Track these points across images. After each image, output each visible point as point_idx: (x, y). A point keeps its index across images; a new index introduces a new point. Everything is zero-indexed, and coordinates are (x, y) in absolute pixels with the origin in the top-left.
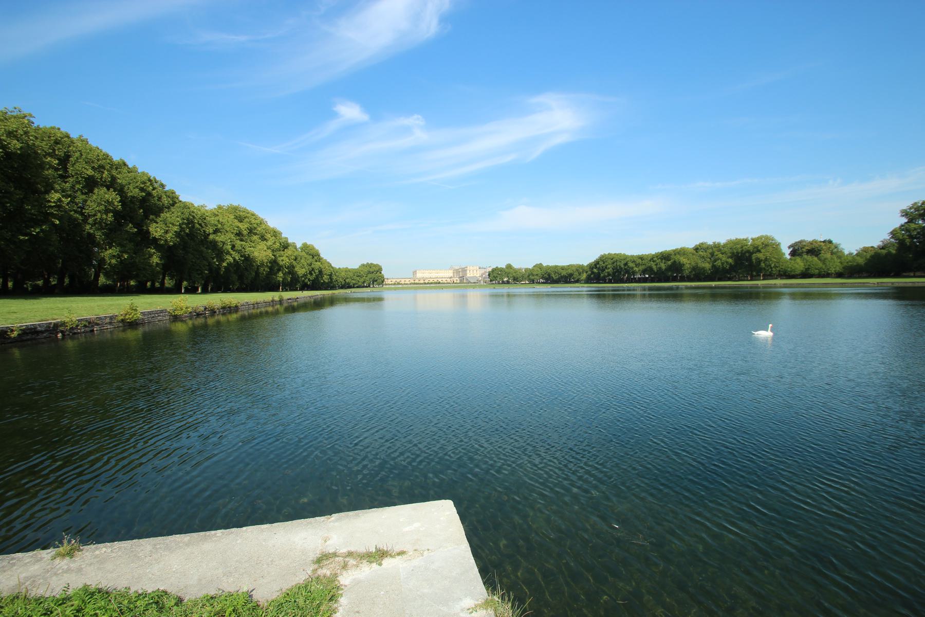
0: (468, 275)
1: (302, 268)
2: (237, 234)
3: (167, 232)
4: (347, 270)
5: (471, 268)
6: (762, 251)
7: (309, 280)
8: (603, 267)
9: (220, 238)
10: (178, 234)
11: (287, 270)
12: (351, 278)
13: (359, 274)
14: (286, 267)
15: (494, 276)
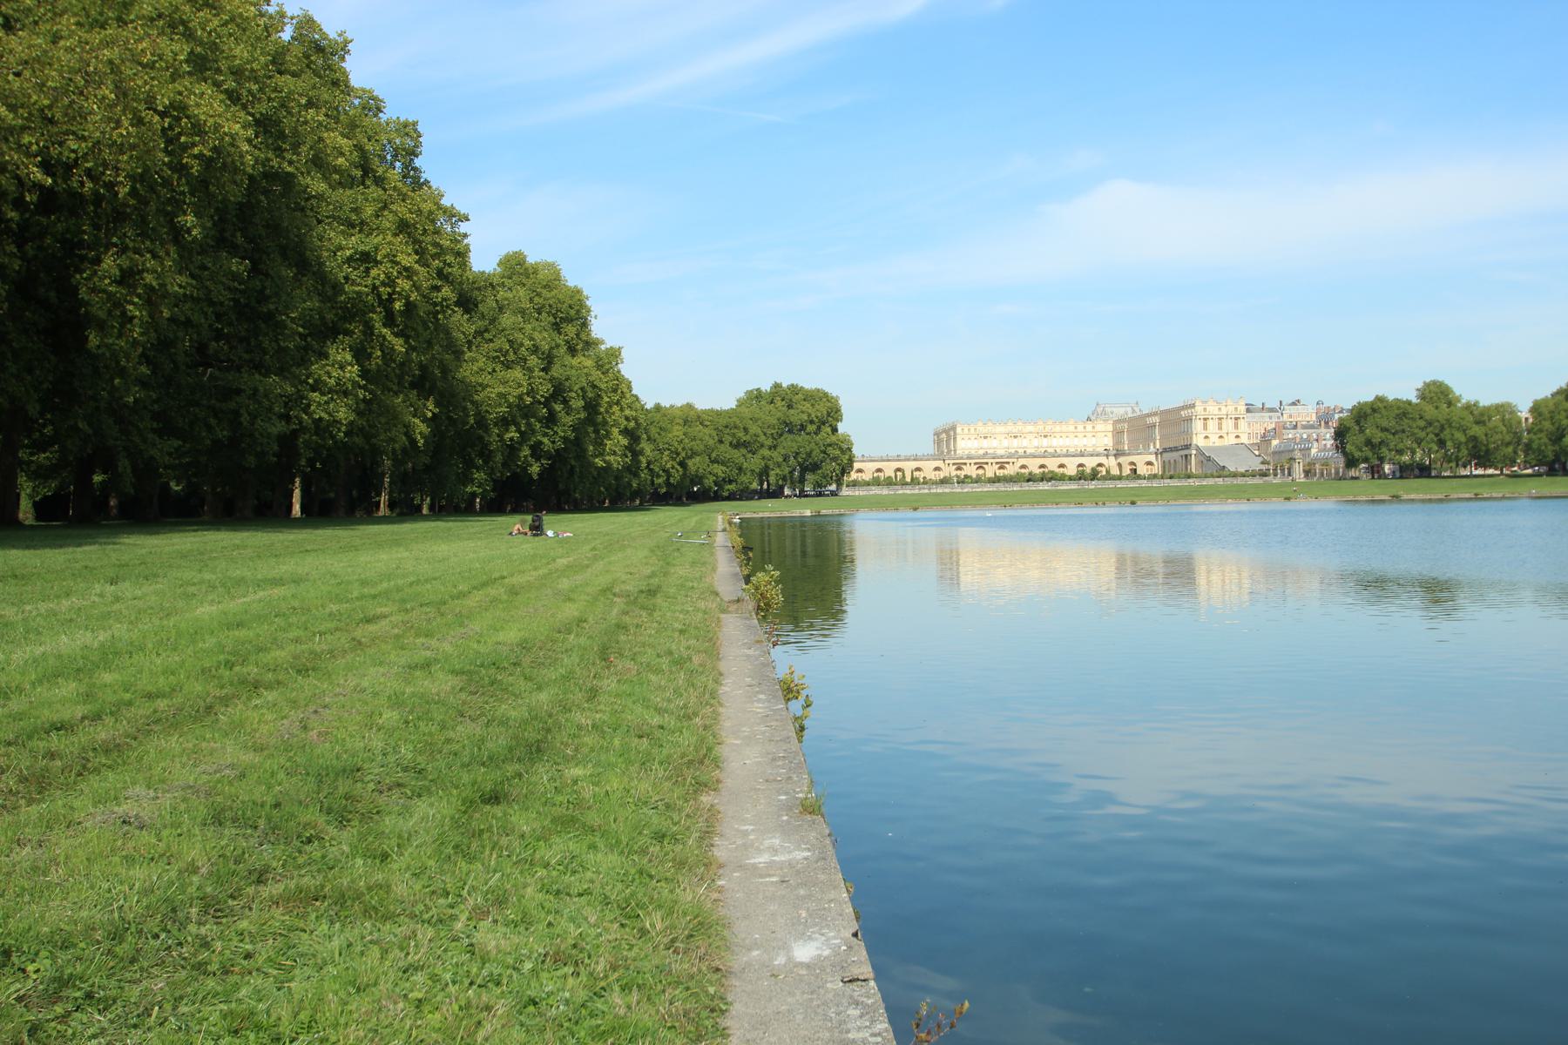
1: (508, 366)
4: (690, 417)
11: (399, 345)
12: (708, 451)
13: (741, 434)
14: (390, 320)
15: (1369, 443)
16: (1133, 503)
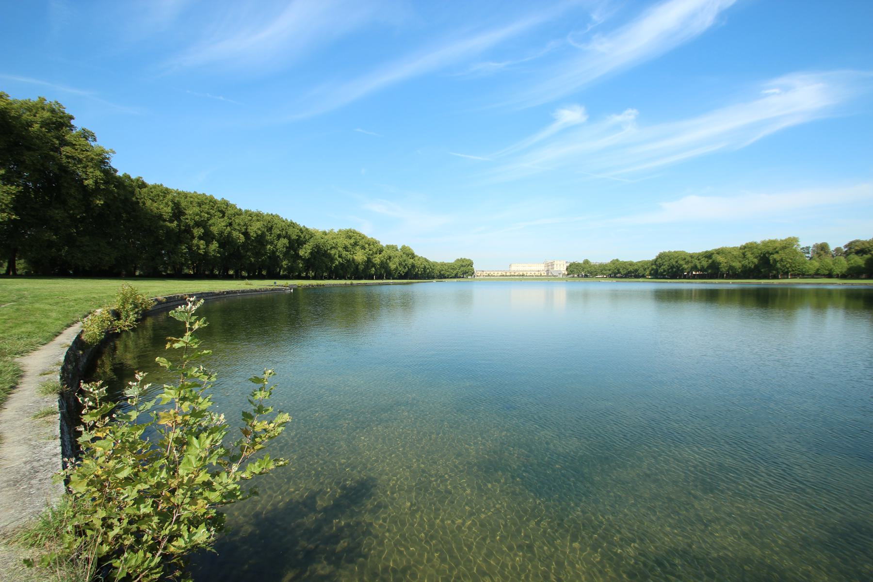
0: (555, 269)
2: (344, 248)
3: (306, 253)
4: (443, 264)
5: (559, 262)
6: (780, 252)
7: (403, 272)
8: (660, 264)
9: (333, 252)
10: (311, 253)
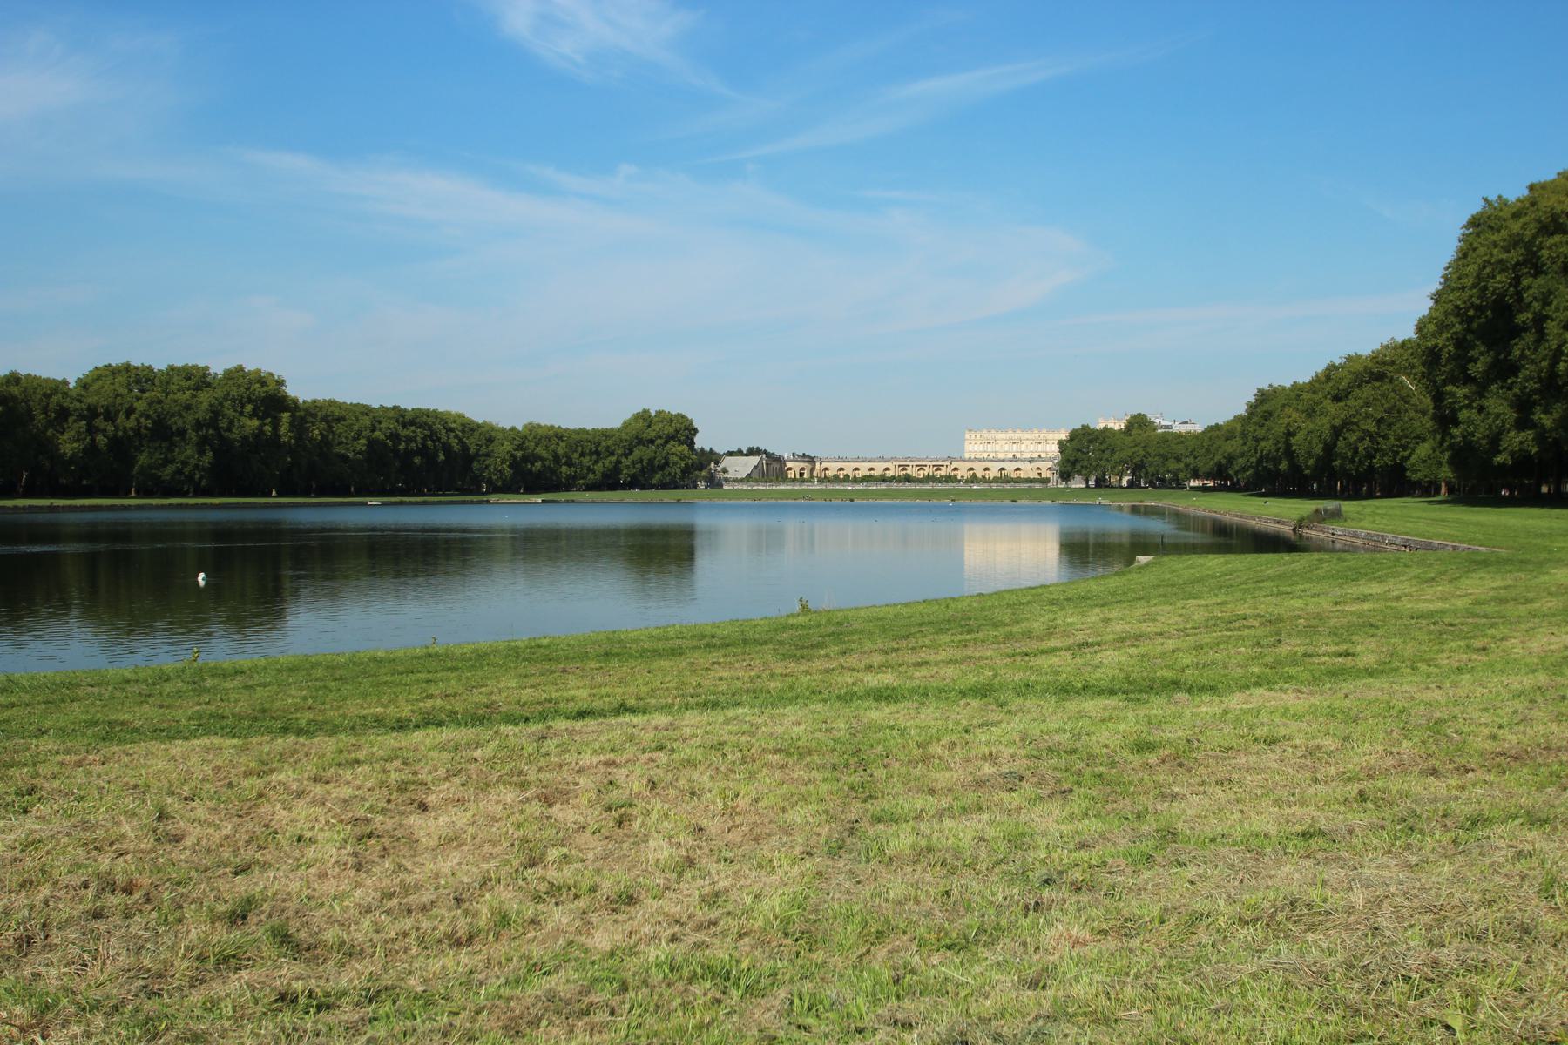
16: (852, 500)
